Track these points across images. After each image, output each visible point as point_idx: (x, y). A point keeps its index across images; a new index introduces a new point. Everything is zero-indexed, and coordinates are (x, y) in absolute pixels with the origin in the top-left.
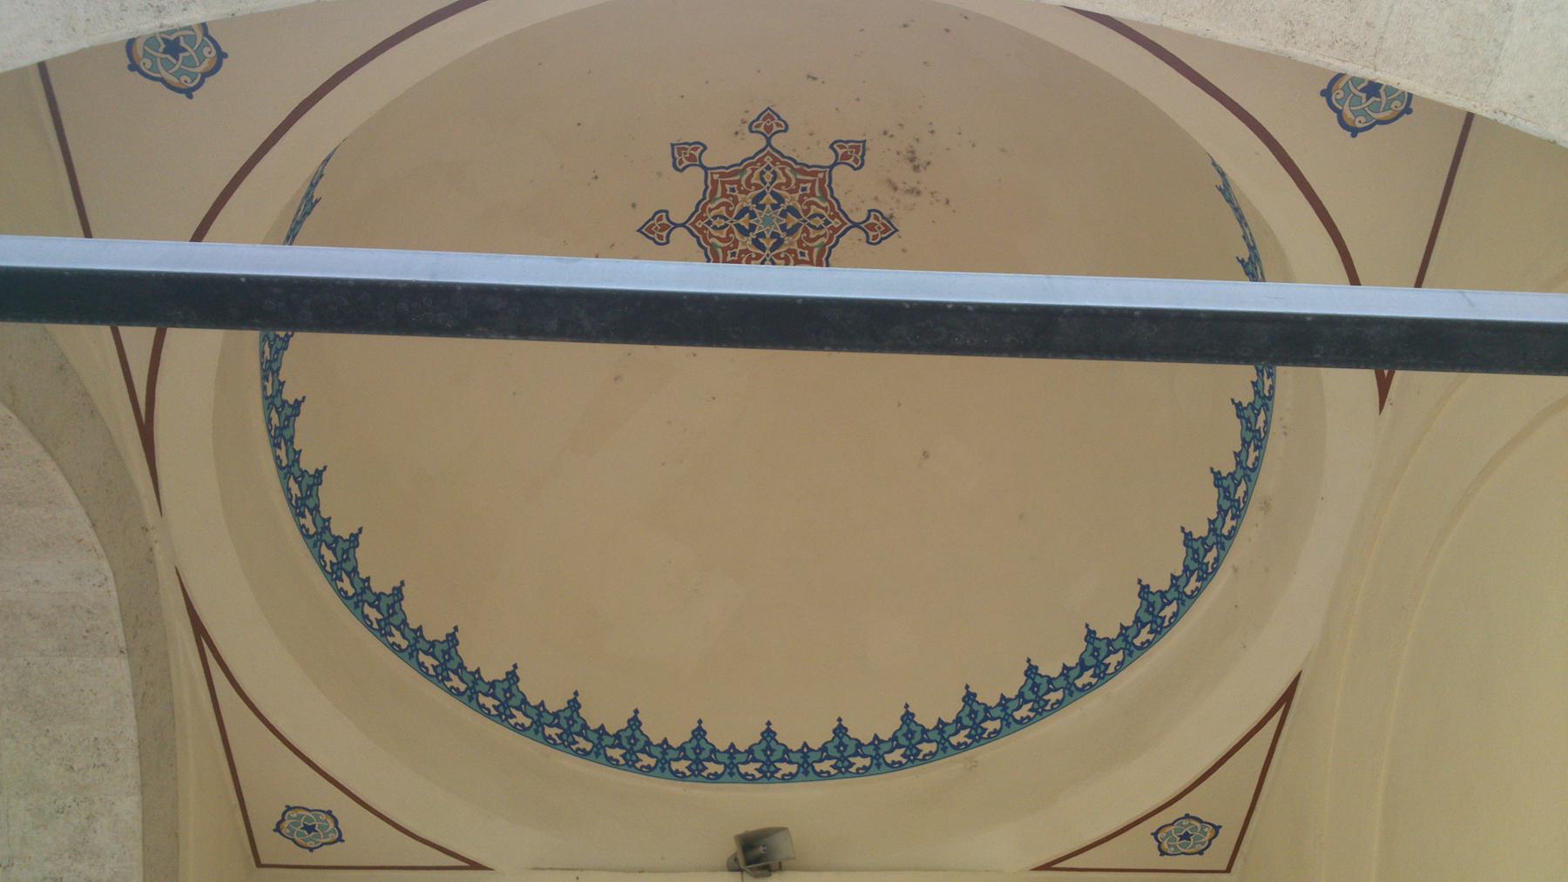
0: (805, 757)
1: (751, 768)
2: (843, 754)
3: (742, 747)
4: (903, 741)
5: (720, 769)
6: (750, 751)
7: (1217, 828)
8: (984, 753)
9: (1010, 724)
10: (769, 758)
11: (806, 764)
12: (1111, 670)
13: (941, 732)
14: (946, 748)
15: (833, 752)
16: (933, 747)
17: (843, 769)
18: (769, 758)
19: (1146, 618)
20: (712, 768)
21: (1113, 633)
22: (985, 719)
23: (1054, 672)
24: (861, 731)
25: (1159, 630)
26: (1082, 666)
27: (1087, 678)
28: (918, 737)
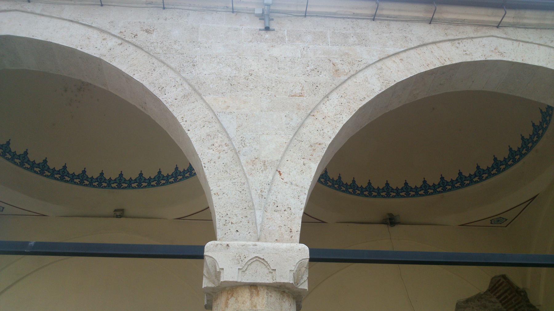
0: (397, 191)
1: (384, 194)
2: (407, 191)
3: (381, 188)
4: (423, 188)
5: (376, 194)
6: (383, 189)
7: (506, 220)
8: (445, 194)
9: (454, 188)
10: (388, 191)
11: (398, 193)
12: (484, 178)
13: (434, 187)
14: (435, 192)
15: (404, 190)
16: (432, 191)
17: (408, 195)
18: (388, 191)
19: (495, 166)
20: (374, 194)
21: (485, 168)
22: (447, 185)
23: (467, 175)
24: (412, 184)
25: (499, 171)
26: (475, 175)
27: (476, 179)
28: (428, 187)
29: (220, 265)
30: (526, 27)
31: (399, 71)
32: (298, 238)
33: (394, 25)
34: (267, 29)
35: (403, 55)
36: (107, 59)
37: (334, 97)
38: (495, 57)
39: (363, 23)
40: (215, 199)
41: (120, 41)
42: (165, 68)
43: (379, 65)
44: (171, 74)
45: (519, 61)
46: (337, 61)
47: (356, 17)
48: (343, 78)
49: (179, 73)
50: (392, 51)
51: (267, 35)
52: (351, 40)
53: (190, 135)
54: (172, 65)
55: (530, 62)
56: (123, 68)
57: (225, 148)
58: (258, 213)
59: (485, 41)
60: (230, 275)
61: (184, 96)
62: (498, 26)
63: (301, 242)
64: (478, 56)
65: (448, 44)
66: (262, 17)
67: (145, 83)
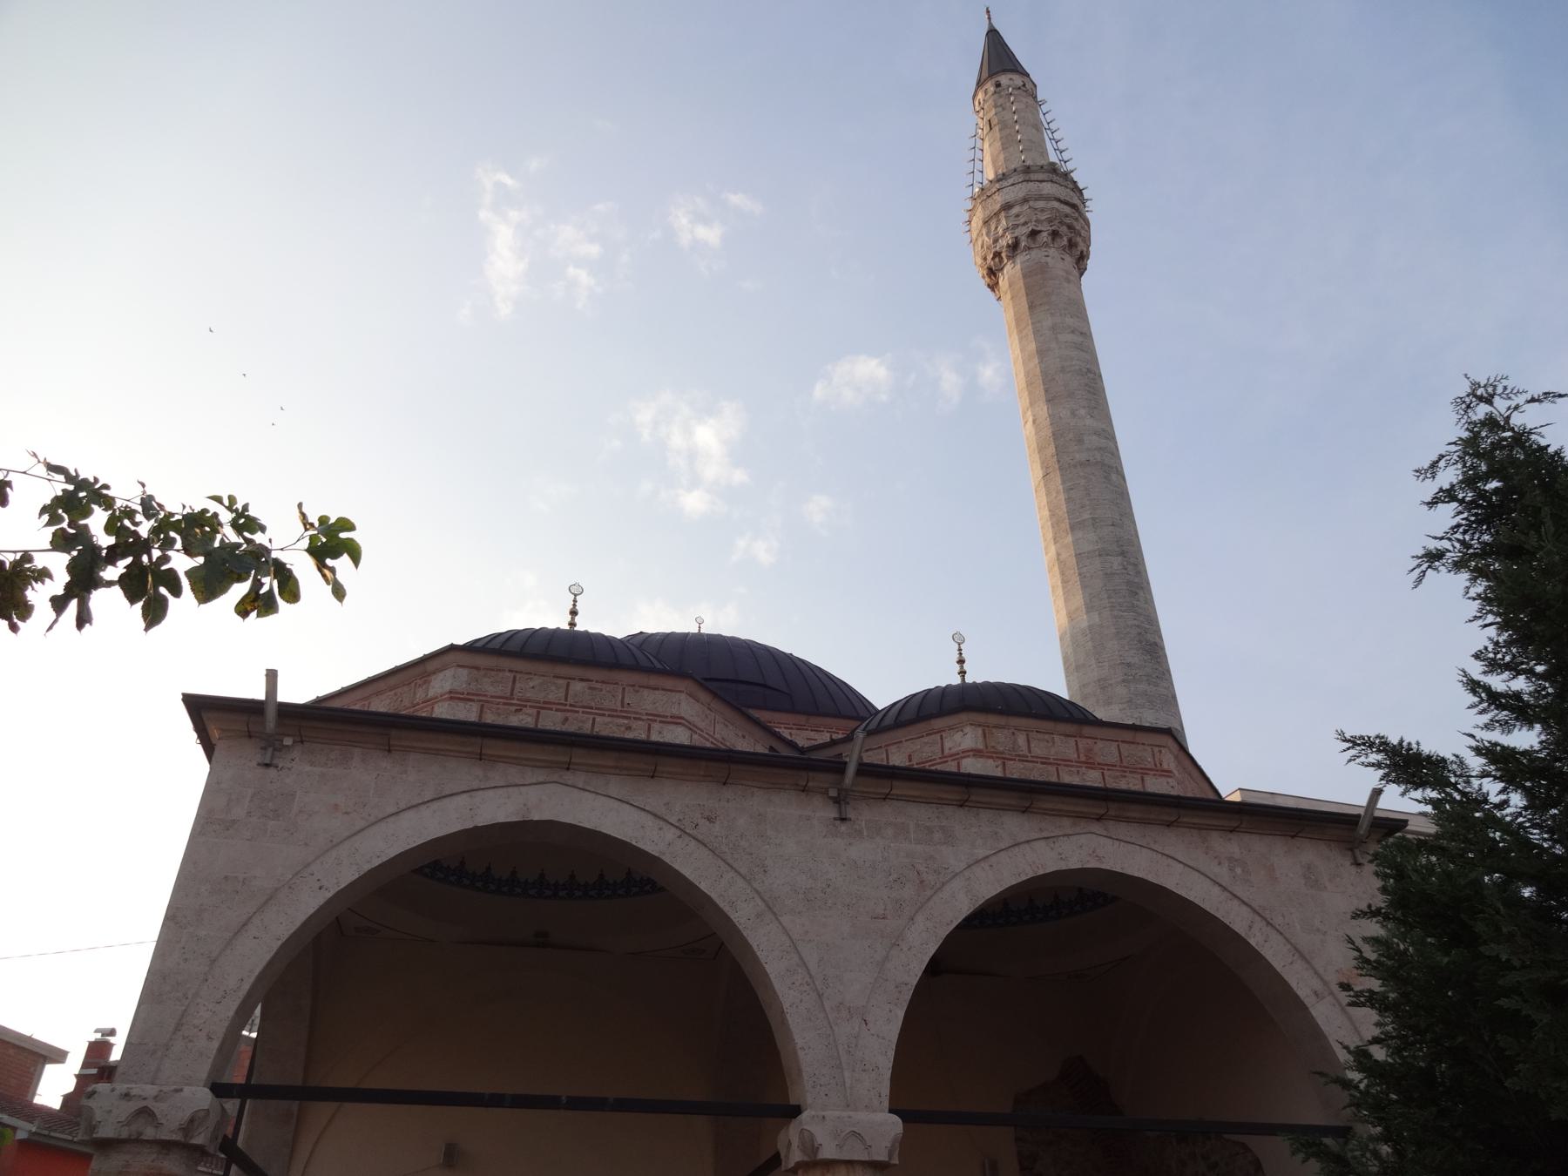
29: (819, 1139)
30: (1128, 820)
31: (989, 884)
32: (886, 1104)
33: (985, 815)
34: (843, 820)
35: (993, 859)
36: (667, 859)
37: (920, 918)
39: (949, 810)
40: (801, 1054)
41: (678, 833)
42: (732, 874)
43: (966, 873)
44: (740, 883)
45: (1118, 869)
46: (922, 869)
47: (941, 802)
48: (929, 893)
49: (749, 882)
50: (981, 852)
51: (843, 828)
52: (937, 836)
53: (768, 968)
54: (742, 871)
55: (1129, 872)
56: (687, 872)
57: (806, 988)
58: (847, 1074)
59: (1083, 839)
60: (828, 1152)
61: (758, 916)
62: (1099, 819)
63: (891, 1111)
64: (1074, 864)
65: (1042, 843)
66: (837, 801)
67: (714, 896)
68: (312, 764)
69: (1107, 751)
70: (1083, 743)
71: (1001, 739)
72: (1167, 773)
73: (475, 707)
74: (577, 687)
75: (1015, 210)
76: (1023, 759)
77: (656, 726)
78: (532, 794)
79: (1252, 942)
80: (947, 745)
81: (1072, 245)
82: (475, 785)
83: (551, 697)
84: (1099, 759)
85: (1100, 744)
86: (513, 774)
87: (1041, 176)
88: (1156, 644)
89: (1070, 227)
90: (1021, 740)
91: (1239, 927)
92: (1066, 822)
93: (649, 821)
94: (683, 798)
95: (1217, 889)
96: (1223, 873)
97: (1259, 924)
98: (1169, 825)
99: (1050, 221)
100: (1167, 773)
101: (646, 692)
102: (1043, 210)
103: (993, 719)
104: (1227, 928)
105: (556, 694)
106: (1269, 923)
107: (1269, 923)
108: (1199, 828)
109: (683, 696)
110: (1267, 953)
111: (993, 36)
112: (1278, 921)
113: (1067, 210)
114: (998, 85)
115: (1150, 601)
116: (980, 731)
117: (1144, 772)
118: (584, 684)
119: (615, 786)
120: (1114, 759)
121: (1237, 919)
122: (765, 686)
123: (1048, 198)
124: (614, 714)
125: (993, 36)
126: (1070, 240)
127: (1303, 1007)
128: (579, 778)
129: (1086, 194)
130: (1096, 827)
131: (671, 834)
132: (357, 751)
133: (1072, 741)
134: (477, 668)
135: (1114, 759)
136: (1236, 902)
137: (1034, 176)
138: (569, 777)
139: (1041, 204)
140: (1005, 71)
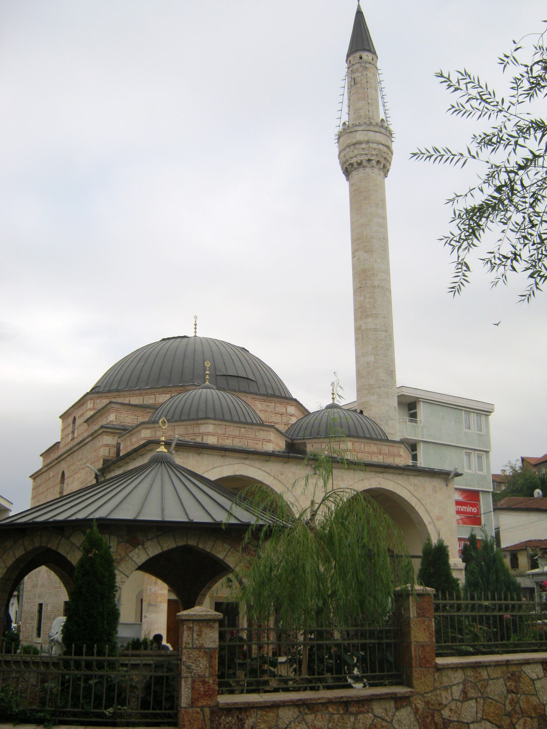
30: (390, 473)
38: (379, 486)
52: (340, 478)
62: (382, 473)
68: (180, 458)
69: (385, 449)
70: (379, 447)
71: (357, 445)
72: (401, 456)
73: (216, 438)
74: (243, 430)
75: (364, 146)
76: (362, 452)
77: (264, 443)
78: (236, 467)
79: (416, 508)
80: (341, 446)
81: (384, 166)
82: (222, 464)
83: (236, 434)
84: (383, 452)
85: (384, 447)
86: (231, 461)
87: (377, 129)
88: (393, 371)
89: (385, 159)
90: (362, 446)
91: (413, 504)
92: (373, 474)
93: (266, 475)
94: (275, 467)
95: (409, 493)
96: (411, 488)
97: (419, 503)
98: (400, 474)
99: (377, 155)
100: (401, 456)
101: (261, 432)
102: (375, 149)
103: (356, 439)
104: (410, 504)
105: (237, 433)
106: (421, 503)
107: (421, 503)
108: (407, 475)
109: (271, 433)
110: (419, 511)
111: (359, 15)
112: (423, 502)
113: (385, 149)
114: (361, 58)
115: (393, 352)
116: (351, 443)
117: (394, 456)
118: (245, 429)
119: (257, 464)
120: (387, 452)
121: (413, 502)
122: (248, 378)
123: (378, 143)
124: (253, 439)
125: (359, 15)
126: (384, 165)
127: (424, 525)
128: (247, 462)
129: (393, 135)
130: (381, 475)
131: (272, 478)
132: (190, 454)
133: (376, 446)
134: (215, 424)
135: (387, 452)
136: (414, 497)
137: (372, 128)
138: (245, 461)
139: (374, 146)
140: (364, 50)
